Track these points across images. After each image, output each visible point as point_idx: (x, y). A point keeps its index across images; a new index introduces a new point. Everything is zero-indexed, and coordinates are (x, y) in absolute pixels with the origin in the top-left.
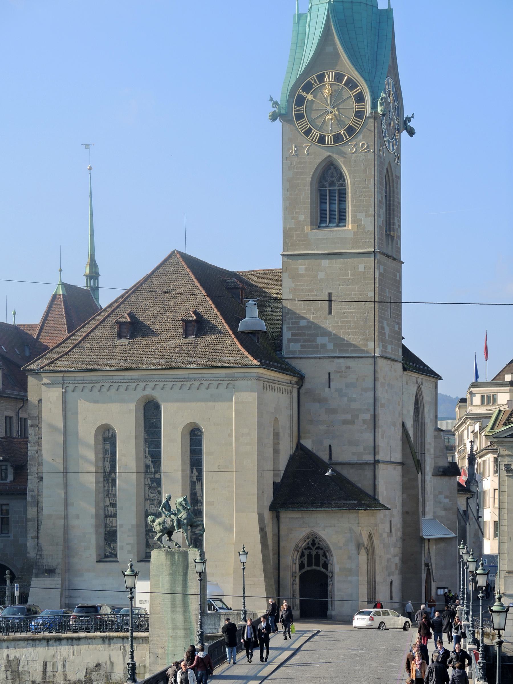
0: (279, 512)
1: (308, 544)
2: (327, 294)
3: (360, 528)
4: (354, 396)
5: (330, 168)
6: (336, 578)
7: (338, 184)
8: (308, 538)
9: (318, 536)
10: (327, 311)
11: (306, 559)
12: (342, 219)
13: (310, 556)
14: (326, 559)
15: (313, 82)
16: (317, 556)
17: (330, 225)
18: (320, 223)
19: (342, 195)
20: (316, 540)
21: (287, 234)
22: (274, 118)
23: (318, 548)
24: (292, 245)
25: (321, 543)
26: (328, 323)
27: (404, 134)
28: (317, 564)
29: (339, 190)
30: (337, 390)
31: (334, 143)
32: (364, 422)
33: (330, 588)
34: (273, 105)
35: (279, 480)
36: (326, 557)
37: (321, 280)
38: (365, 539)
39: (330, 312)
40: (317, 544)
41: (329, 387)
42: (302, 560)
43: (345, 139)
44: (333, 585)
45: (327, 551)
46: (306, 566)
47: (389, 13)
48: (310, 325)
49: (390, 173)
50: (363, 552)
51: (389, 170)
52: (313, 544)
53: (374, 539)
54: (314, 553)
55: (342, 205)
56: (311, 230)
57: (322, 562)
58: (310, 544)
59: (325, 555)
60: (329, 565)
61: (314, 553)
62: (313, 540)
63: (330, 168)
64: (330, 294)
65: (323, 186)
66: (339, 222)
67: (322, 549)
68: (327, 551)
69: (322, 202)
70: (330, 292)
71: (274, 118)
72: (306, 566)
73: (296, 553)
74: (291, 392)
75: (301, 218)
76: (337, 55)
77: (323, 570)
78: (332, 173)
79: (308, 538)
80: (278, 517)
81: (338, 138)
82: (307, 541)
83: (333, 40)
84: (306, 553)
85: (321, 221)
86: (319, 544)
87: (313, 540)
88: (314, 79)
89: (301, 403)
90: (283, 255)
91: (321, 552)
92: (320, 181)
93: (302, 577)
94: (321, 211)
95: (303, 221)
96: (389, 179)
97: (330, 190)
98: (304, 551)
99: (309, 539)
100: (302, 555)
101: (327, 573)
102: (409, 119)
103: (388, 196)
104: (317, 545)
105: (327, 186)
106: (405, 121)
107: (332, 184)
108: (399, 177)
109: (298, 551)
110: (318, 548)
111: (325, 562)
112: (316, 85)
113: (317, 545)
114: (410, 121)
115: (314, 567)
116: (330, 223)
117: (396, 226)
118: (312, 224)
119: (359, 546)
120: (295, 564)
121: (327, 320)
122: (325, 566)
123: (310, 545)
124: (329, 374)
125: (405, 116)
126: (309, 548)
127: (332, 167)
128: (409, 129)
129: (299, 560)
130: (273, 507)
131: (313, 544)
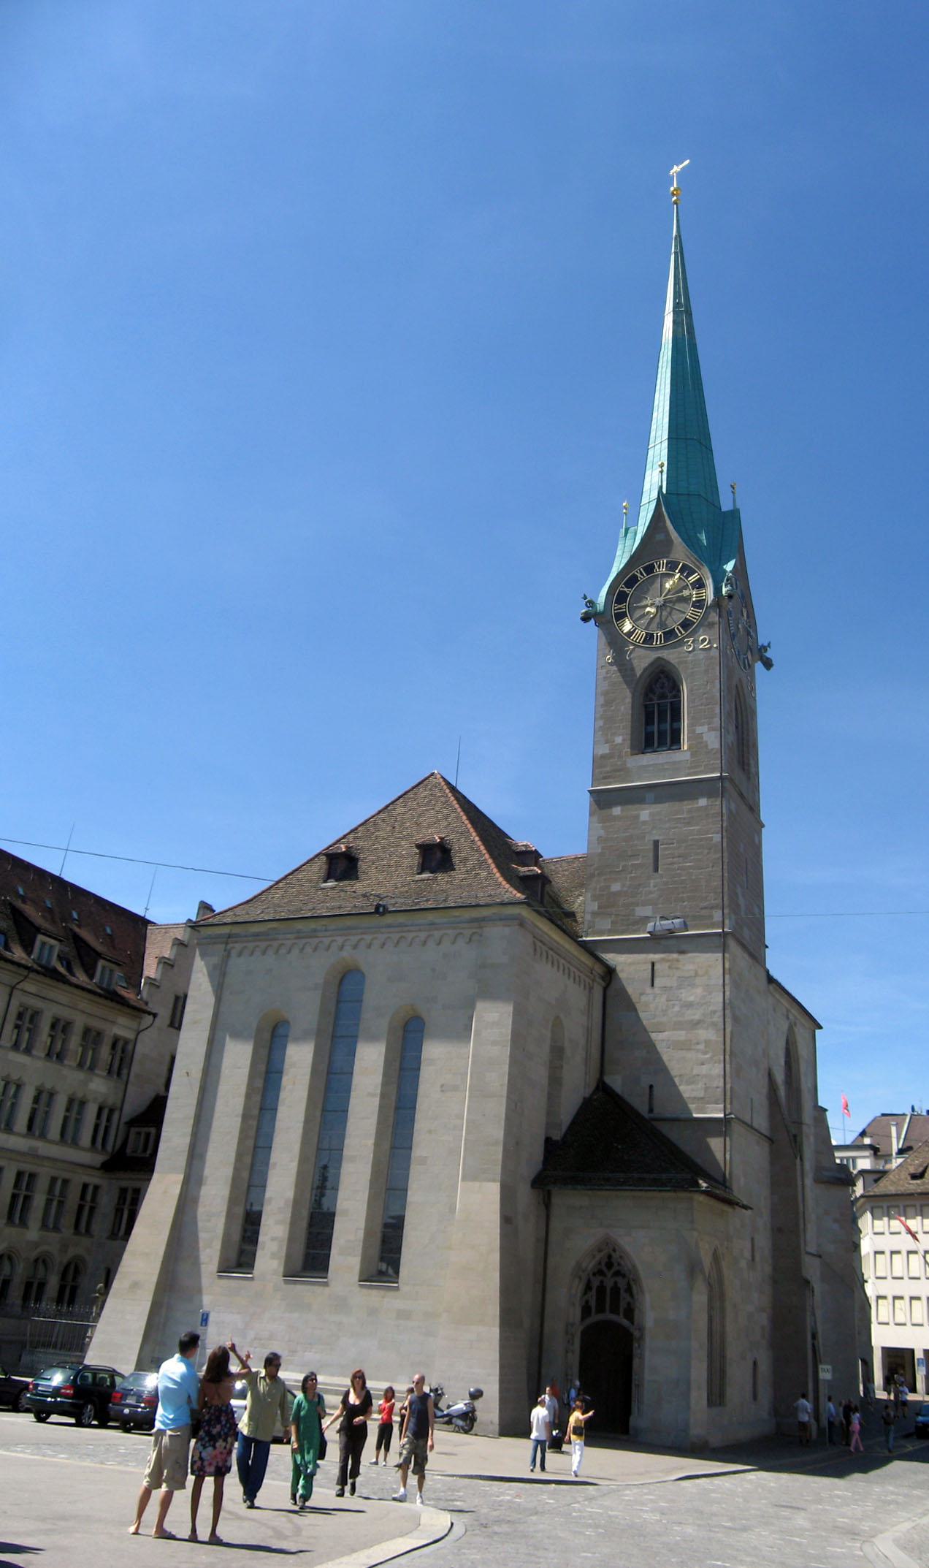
0: (549, 1193)
1: (600, 1263)
2: (652, 842)
3: (695, 1234)
4: (692, 998)
5: (660, 678)
6: (649, 1342)
7: (669, 695)
8: (600, 1251)
9: (616, 1247)
10: (651, 868)
11: (594, 1298)
12: (675, 741)
13: (601, 1289)
14: (629, 1299)
15: (639, 575)
16: (616, 1290)
17: (658, 750)
18: (645, 748)
19: (676, 716)
20: (613, 1254)
21: (598, 762)
22: (586, 618)
23: (618, 1273)
24: (605, 778)
25: (622, 1262)
26: (652, 885)
27: (759, 666)
28: (615, 1310)
29: (671, 703)
30: (665, 988)
31: (665, 642)
32: (707, 1042)
33: (636, 1362)
34: (586, 603)
35: (557, 1136)
36: (632, 1295)
37: (644, 823)
38: (707, 1261)
39: (656, 870)
40: (616, 1264)
41: (653, 985)
42: (586, 1297)
43: (679, 635)
44: (642, 1357)
45: (633, 1280)
46: (593, 1310)
47: (735, 514)
48: (625, 889)
49: (741, 694)
50: (701, 1286)
51: (740, 689)
52: (609, 1265)
53: (724, 1264)
54: (609, 1283)
55: (675, 725)
56: (632, 755)
57: (623, 1305)
58: (603, 1264)
59: (629, 1290)
60: (636, 1312)
61: (609, 1283)
62: (610, 1257)
63: (660, 678)
64: (656, 843)
65: (651, 700)
66: (671, 746)
67: (624, 1276)
68: (633, 1280)
69: (649, 720)
70: (657, 838)
71: (586, 618)
72: (593, 1310)
73: (577, 1281)
74: (591, 989)
75: (619, 740)
76: (669, 542)
77: (625, 1322)
78: (663, 684)
79: (600, 1251)
80: (547, 1205)
81: (669, 634)
82: (598, 1258)
83: (665, 527)
84: (595, 1283)
85: (645, 747)
86: (619, 1264)
87: (610, 1257)
88: (641, 572)
89: (609, 1010)
90: (590, 792)
91: (622, 1283)
92: (646, 695)
93: (584, 1333)
94: (647, 734)
95: (621, 744)
96: (740, 702)
97: (658, 704)
98: (592, 1278)
99: (602, 1254)
100: (588, 1287)
101: (632, 1330)
102: (765, 648)
103: (740, 727)
104: (615, 1268)
105: (655, 698)
106: (760, 650)
107: (663, 696)
108: (754, 713)
109: (580, 1278)
110: (618, 1273)
111: (629, 1304)
112: (642, 577)
113: (615, 1268)
114: (766, 651)
115: (609, 1316)
116: (658, 747)
117: (753, 770)
118: (632, 747)
119: (693, 1269)
120: (574, 1304)
121: (652, 881)
122: (629, 1313)
123: (604, 1269)
124: (653, 964)
125: (760, 644)
126: (600, 1272)
127: (662, 676)
128: (764, 659)
129: (581, 1299)
130: (541, 1182)
131: (609, 1265)
